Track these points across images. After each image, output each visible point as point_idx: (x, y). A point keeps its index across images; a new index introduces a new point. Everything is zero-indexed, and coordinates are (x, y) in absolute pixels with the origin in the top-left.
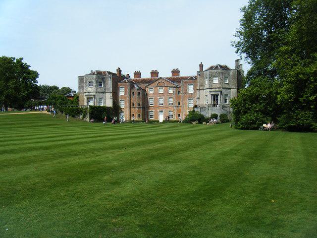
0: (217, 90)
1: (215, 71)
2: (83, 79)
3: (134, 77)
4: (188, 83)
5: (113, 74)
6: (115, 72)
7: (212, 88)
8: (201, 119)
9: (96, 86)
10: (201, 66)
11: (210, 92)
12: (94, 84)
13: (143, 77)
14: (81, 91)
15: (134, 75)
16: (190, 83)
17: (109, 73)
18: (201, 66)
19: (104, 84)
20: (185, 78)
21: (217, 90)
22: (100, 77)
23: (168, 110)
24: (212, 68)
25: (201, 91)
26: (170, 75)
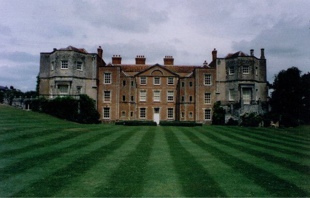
2: (49, 57)
9: (74, 68)
11: (240, 85)
12: (70, 64)
13: (124, 62)
14: (44, 75)
19: (84, 66)
21: (249, 82)
22: (79, 56)
23: (167, 107)
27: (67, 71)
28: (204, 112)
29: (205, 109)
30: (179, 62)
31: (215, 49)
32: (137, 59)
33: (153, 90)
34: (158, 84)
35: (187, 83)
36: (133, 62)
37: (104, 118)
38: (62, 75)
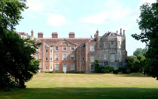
0: (114, 50)
4: (90, 44)
7: (110, 49)
10: (97, 32)
16: (92, 44)
18: (97, 32)
25: (100, 51)
26: (67, 37)
30: (77, 37)
32: (53, 35)
33: (63, 54)
34: (65, 50)
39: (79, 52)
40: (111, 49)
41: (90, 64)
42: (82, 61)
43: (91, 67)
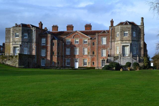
0: (127, 42)
1: (126, 26)
2: (10, 30)
3: (52, 30)
4: (101, 35)
5: (36, 27)
6: (38, 26)
7: (123, 41)
8: (118, 67)
10: (112, 22)
13: (60, 30)
15: (53, 28)
17: (33, 26)
18: (112, 22)
20: (99, 32)
24: (121, 24)
26: (84, 29)
27: (18, 39)
28: (101, 61)
29: (102, 59)
31: (112, 19)
32: (68, 27)
35: (91, 44)
36: (65, 30)
37: (42, 65)
38: (15, 41)
39: (89, 45)
40: (124, 41)
41: (101, 60)
42: (92, 56)
43: (102, 62)
